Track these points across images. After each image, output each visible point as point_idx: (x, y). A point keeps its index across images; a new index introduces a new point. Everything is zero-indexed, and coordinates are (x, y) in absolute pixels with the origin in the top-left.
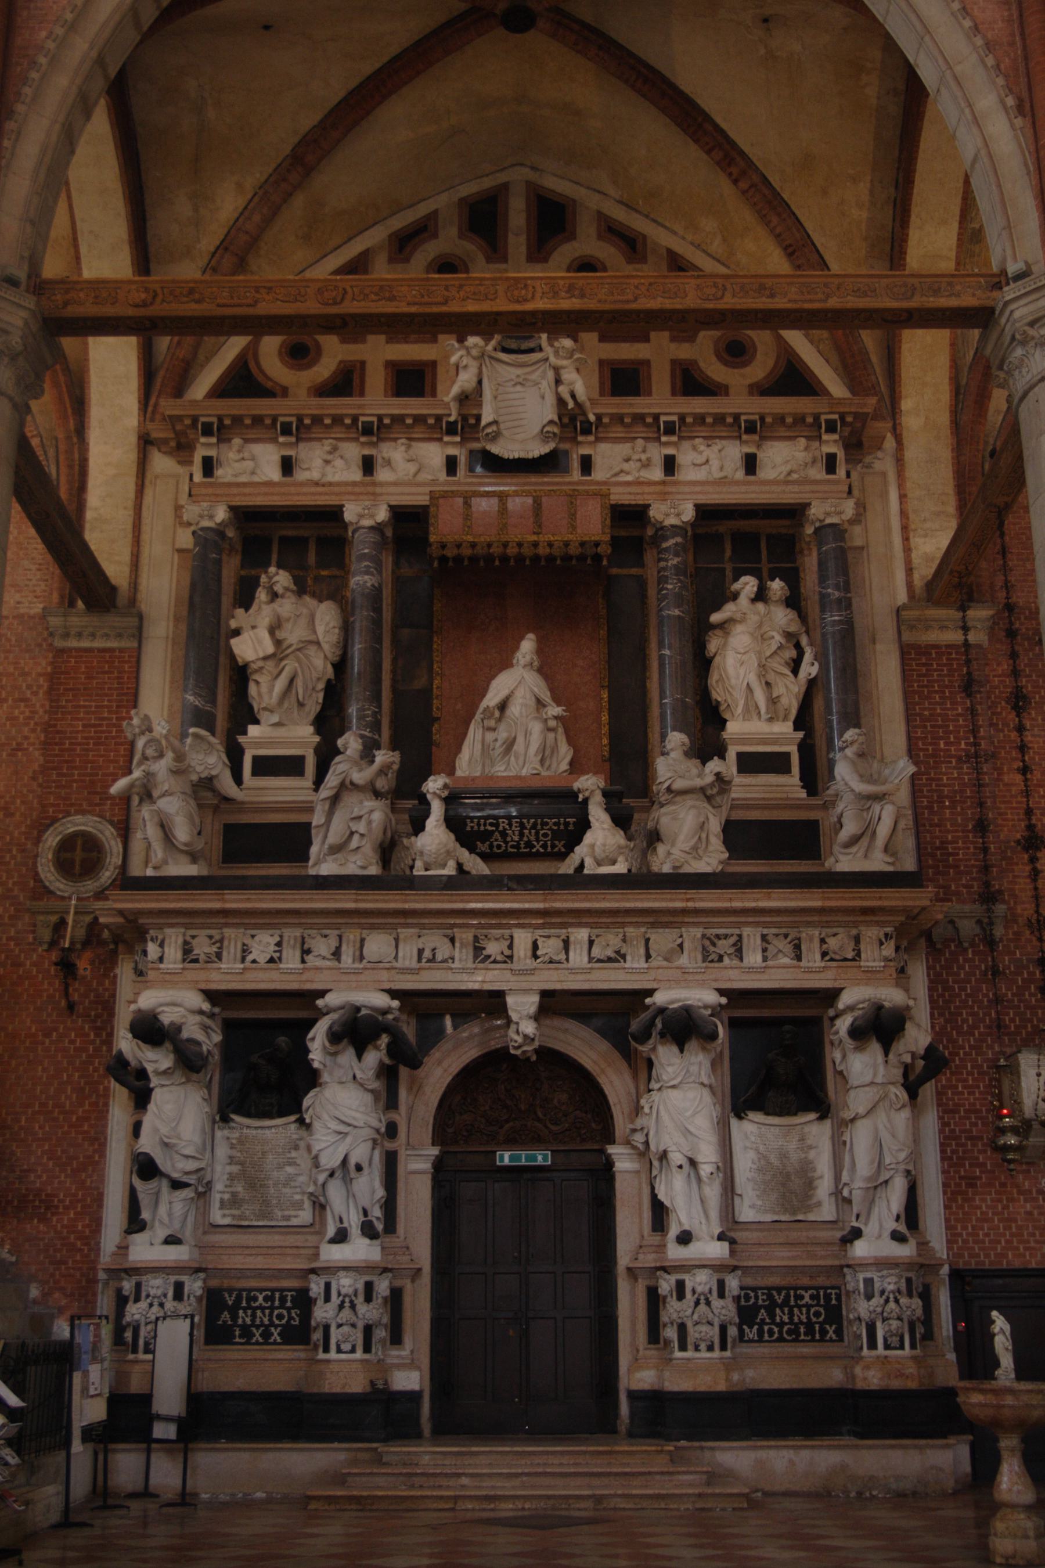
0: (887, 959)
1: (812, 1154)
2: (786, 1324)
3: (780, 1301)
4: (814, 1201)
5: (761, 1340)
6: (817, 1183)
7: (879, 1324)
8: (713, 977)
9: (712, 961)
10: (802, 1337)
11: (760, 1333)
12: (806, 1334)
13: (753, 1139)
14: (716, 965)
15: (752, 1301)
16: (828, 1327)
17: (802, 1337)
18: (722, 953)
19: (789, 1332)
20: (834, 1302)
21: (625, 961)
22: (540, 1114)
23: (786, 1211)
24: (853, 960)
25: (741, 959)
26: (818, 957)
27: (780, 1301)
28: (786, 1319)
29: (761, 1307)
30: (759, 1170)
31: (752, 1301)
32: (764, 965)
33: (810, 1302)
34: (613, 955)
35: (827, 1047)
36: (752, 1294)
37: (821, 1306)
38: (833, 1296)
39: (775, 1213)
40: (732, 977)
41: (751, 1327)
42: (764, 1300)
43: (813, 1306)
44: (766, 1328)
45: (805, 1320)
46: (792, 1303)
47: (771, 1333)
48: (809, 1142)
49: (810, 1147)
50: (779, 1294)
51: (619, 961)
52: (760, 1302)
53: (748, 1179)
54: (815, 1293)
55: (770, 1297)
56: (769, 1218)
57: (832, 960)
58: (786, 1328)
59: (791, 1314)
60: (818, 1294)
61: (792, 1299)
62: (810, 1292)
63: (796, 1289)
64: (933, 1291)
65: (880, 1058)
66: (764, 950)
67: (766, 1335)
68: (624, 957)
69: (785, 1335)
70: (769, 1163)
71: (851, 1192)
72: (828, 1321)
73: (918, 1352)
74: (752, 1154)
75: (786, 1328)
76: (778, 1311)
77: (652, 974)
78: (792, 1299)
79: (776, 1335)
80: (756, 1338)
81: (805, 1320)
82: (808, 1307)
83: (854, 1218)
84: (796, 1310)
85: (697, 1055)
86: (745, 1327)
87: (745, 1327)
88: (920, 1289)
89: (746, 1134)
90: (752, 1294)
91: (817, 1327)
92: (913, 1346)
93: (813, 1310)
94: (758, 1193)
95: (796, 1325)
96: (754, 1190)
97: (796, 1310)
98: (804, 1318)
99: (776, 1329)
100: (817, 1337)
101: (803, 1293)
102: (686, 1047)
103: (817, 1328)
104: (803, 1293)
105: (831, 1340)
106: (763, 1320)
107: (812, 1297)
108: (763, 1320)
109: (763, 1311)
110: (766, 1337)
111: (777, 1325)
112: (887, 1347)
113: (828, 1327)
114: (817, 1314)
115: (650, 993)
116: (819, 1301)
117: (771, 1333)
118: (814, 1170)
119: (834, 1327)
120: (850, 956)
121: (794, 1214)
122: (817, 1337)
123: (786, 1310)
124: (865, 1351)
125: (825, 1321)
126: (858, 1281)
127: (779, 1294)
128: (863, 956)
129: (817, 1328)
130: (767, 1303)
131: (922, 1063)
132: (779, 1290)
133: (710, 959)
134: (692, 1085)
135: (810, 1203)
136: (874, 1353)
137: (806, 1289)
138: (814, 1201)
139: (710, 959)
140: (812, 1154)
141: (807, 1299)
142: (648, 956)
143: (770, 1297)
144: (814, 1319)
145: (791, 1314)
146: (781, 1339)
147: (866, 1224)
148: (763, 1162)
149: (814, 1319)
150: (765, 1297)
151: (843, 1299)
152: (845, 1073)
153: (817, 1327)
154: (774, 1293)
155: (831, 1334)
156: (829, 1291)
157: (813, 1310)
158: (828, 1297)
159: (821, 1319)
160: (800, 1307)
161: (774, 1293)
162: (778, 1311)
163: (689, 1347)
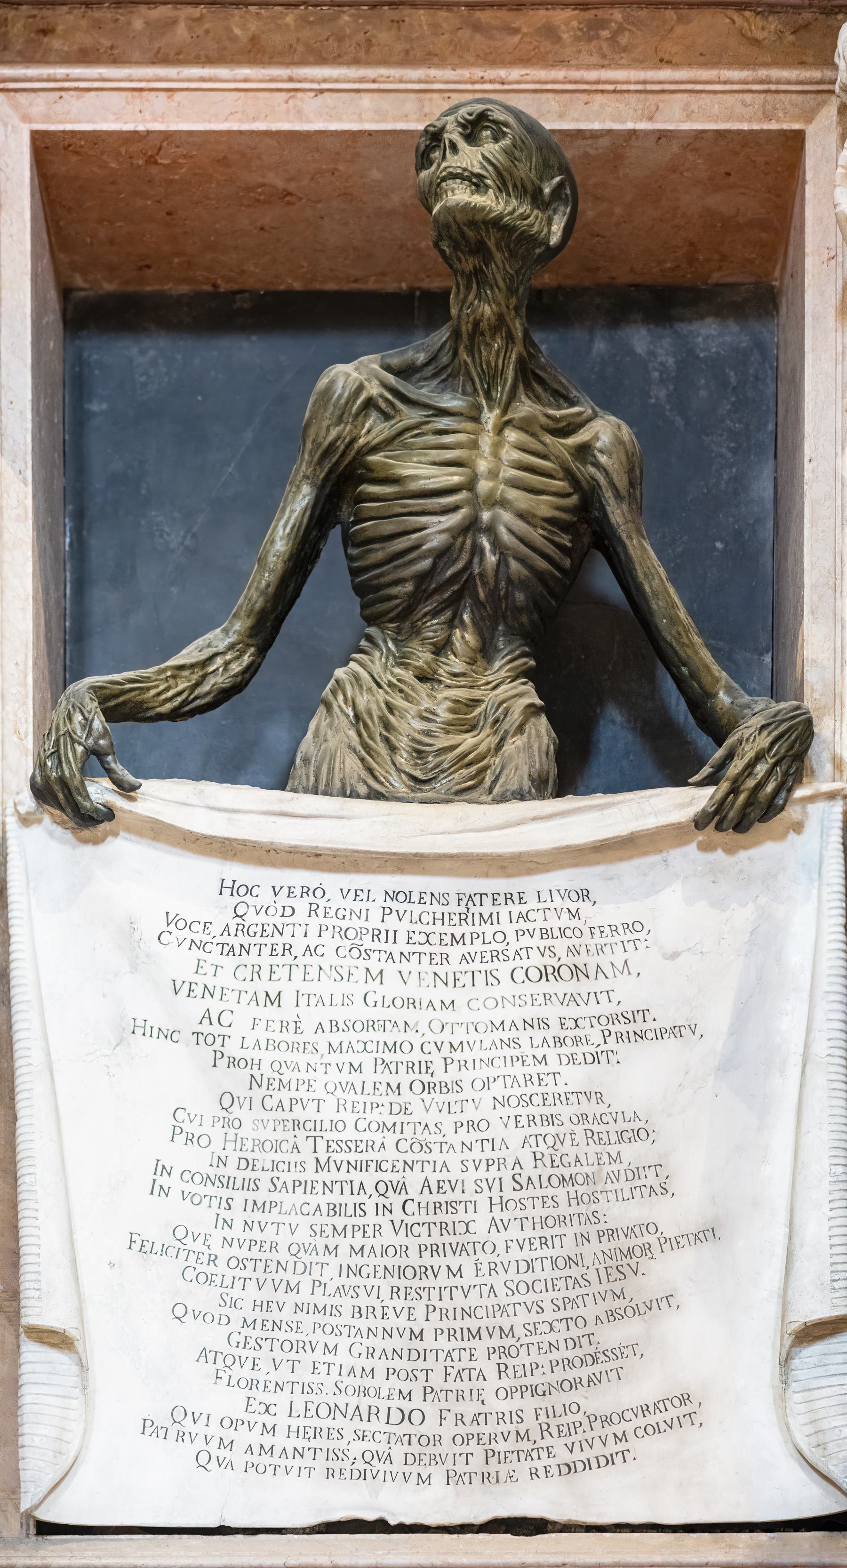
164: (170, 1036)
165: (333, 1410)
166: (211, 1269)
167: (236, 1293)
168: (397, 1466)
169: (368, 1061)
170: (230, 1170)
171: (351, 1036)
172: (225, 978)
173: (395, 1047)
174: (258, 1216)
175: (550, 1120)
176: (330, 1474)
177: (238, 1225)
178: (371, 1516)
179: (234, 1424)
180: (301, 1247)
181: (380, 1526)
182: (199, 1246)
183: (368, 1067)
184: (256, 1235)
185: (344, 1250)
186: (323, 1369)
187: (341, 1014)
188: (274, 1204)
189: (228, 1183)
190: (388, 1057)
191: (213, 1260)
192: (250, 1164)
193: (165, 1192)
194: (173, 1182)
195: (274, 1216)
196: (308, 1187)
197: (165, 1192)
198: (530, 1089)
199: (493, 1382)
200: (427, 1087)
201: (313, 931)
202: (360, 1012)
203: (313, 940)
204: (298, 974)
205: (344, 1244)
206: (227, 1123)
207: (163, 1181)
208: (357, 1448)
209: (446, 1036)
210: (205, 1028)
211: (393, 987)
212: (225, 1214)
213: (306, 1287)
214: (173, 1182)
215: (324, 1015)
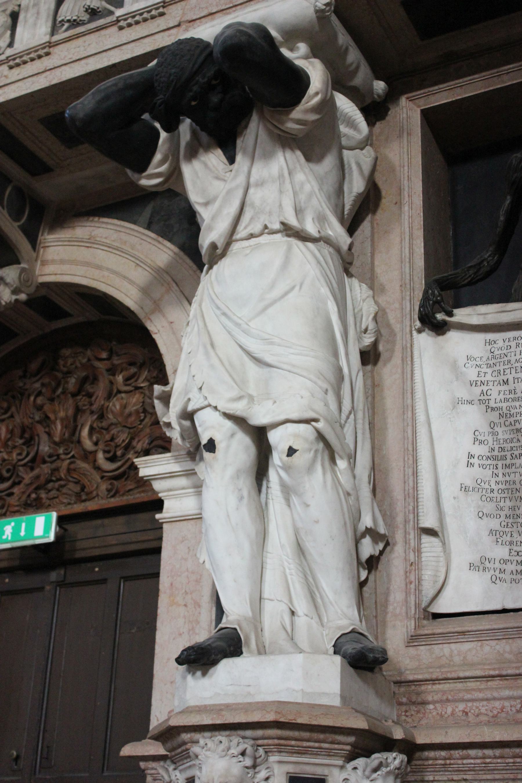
13: (472, 374)
22: (88, 444)
53: (465, 489)
85: (268, 156)
89: (454, 366)
94: (495, 524)
96: (481, 515)
102: (239, 142)
134: (265, 239)
148: (502, 433)
164: (470, 402)
167: (502, 504)
170: (496, 453)
172: (489, 377)
174: (507, 470)
177: (501, 475)
179: (505, 562)
182: (486, 486)
184: (507, 478)
188: (513, 465)
189: (495, 458)
191: (492, 491)
192: (502, 449)
193: (472, 465)
194: (475, 461)
195: (513, 469)
197: (472, 465)
204: (513, 371)
206: (493, 434)
207: (472, 461)
210: (482, 398)
212: (495, 471)
214: (475, 461)
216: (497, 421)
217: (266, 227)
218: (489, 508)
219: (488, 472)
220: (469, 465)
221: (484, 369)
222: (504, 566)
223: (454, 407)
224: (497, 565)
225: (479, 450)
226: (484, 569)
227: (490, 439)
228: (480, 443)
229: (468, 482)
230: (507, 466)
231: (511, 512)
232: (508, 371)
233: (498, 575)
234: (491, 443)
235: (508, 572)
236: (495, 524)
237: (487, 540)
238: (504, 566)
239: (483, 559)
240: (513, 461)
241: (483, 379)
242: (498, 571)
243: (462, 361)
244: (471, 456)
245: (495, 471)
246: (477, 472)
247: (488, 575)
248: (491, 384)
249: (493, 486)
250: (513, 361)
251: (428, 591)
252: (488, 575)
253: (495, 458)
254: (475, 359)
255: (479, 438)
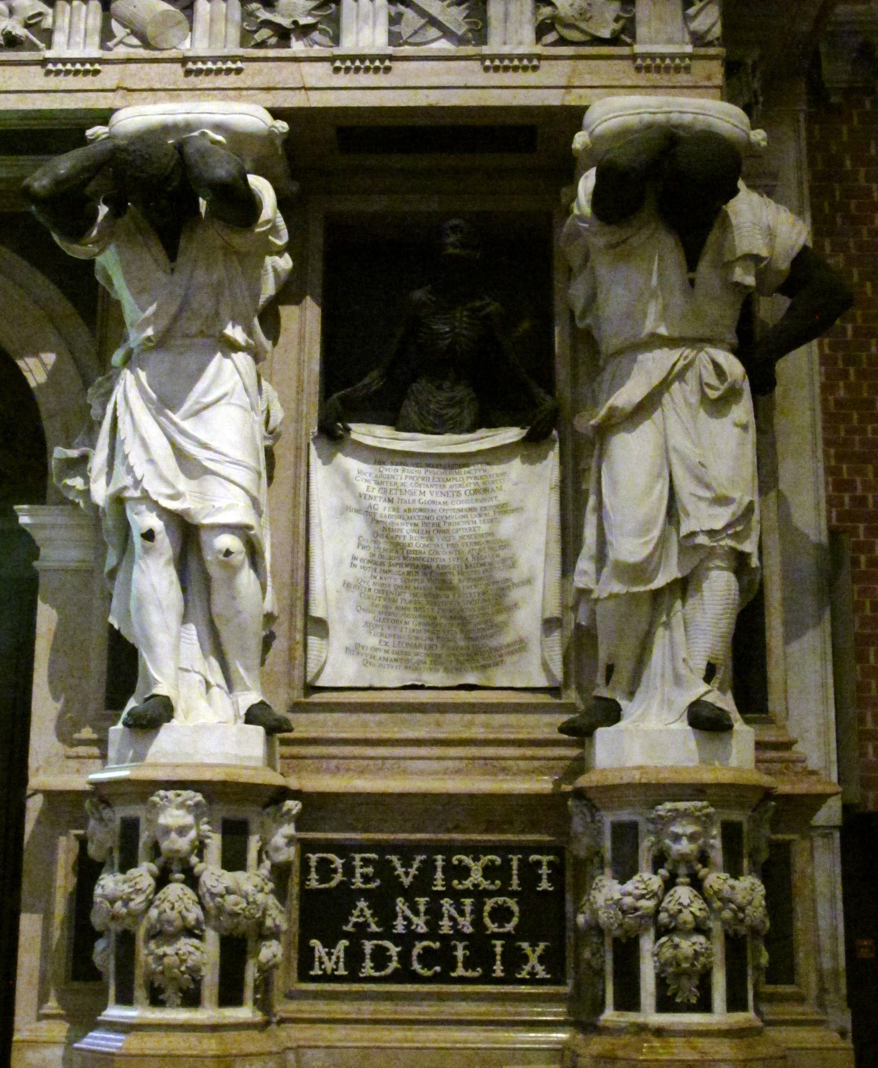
0: (698, 39)
1: (507, 526)
2: (422, 937)
3: (407, 881)
4: (508, 638)
5: (353, 977)
6: (515, 595)
7: (647, 944)
8: (259, 82)
9: (262, 45)
10: (460, 971)
11: (354, 957)
12: (468, 964)
14: (271, 53)
15: (338, 878)
16: (525, 945)
17: (460, 971)
18: (286, 22)
19: (427, 958)
20: (545, 885)
21: (49, 46)
23: (436, 661)
24: (614, 41)
25: (336, 40)
26: (528, 33)
27: (407, 881)
28: (420, 924)
29: (362, 893)
30: (376, 563)
31: (338, 878)
32: (390, 50)
33: (485, 884)
34: (20, 31)
35: (558, 278)
36: (338, 862)
37: (512, 894)
38: (544, 871)
39: (408, 666)
40: (311, 82)
41: (330, 944)
42: (366, 879)
43: (490, 894)
44: (368, 946)
45: (469, 930)
46: (439, 886)
47: (380, 958)
48: (502, 498)
49: (503, 509)
50: (407, 864)
51: (34, 47)
52: (358, 882)
53: (347, 585)
54: (498, 861)
55: (383, 869)
56: (393, 677)
57: (562, 41)
58: (418, 948)
59: (434, 914)
60: (507, 863)
61: (439, 875)
62: (485, 859)
63: (449, 849)
64: (799, 862)
65: (676, 275)
66: (394, 20)
67: (368, 964)
68: (47, 36)
69: (416, 966)
70: (398, 546)
71: (593, 613)
72: (526, 931)
73: (745, 1018)
74: (358, 524)
75: (418, 948)
76: (401, 904)
77: (110, 76)
78: (439, 875)
79: (394, 965)
80: (342, 972)
81: (469, 930)
82: (479, 895)
83: (600, 679)
84: (447, 904)
86: (315, 943)
87: (315, 943)
88: (764, 856)
90: (338, 862)
91: (499, 946)
92: (735, 1003)
93: (489, 904)
94: (369, 617)
95: (445, 939)
96: (359, 609)
97: (447, 904)
98: (466, 925)
99: (394, 950)
100: (498, 970)
101: (467, 860)
103: (499, 950)
104: (467, 860)
105: (533, 980)
106: (362, 927)
107: (489, 872)
108: (362, 927)
109: (362, 904)
110: (368, 969)
111: (397, 939)
112: (664, 1004)
113: (525, 945)
114: (501, 914)
115: (104, 117)
116: (507, 880)
117: (380, 958)
118: (512, 564)
119: (542, 945)
120: (606, 33)
121: (459, 670)
122: (498, 970)
123: (422, 902)
124: (610, 1015)
125: (521, 932)
126: (600, 832)
127: (407, 864)
128: (642, 31)
129: (499, 950)
130: (372, 885)
131: (784, 302)
132: (406, 852)
133: (258, 37)
135: (493, 643)
136: (631, 1017)
137: (476, 850)
138: (508, 638)
139: (258, 37)
140: (507, 526)
141: (476, 876)
142: (107, 34)
143: (383, 869)
144: (493, 927)
145: (434, 914)
146: (405, 975)
147: (631, 694)
148: (383, 544)
149: (493, 927)
150: (370, 870)
151: (569, 874)
152: (595, 332)
153: (499, 946)
154: (395, 859)
155: (534, 964)
156: (534, 858)
157: (489, 904)
158: (529, 872)
159: (509, 927)
160: (457, 896)
161: (395, 859)
162: (401, 904)
163: (140, 993)
165: (407, 644)
166: (369, 593)
167: (377, 602)
168: (427, 666)
169: (420, 522)
170: (376, 558)
171: (415, 514)
173: (428, 518)
174: (385, 575)
175: (476, 544)
176: (406, 667)
177: (378, 578)
178: (419, 683)
179: (376, 649)
180: (398, 586)
181: (422, 687)
182: (365, 585)
183: (420, 525)
184: (383, 581)
185: (412, 587)
186: (404, 630)
187: (412, 506)
188: (390, 571)
190: (426, 521)
191: (370, 590)
192: (382, 556)
193: (355, 566)
194: (357, 562)
195: (390, 575)
196: (401, 565)
197: (355, 566)
198: (472, 533)
199: (459, 636)
200: (439, 531)
201: (404, 477)
202: (418, 506)
203: (403, 481)
204: (398, 493)
205: (412, 585)
206: (375, 542)
207: (355, 562)
208: (416, 658)
209: (444, 514)
210: (369, 510)
211: (428, 497)
212: (374, 574)
213: (399, 601)
214: (357, 562)
215: (406, 506)
216: (380, 532)
217: (202, 332)
218: (366, 603)
219: (368, 574)
220: (353, 565)
221: (373, 485)
222: (375, 653)
223: (342, 514)
224: (368, 651)
225: (362, 554)
226: (358, 653)
227: (372, 545)
228: (363, 548)
229: (351, 580)
230: (386, 572)
231: (384, 610)
232: (394, 492)
233: (369, 660)
234: (372, 550)
235: (378, 658)
236: (369, 617)
237: (362, 630)
238: (375, 653)
239: (357, 646)
240: (392, 568)
241: (370, 493)
242: (368, 657)
243: (353, 473)
244: (354, 558)
245: (374, 574)
246: (358, 572)
247: (360, 659)
248: (378, 499)
249: (371, 587)
250: (399, 484)
251: (312, 668)
252: (360, 659)
253: (376, 563)
254: (365, 474)
255: (363, 543)
